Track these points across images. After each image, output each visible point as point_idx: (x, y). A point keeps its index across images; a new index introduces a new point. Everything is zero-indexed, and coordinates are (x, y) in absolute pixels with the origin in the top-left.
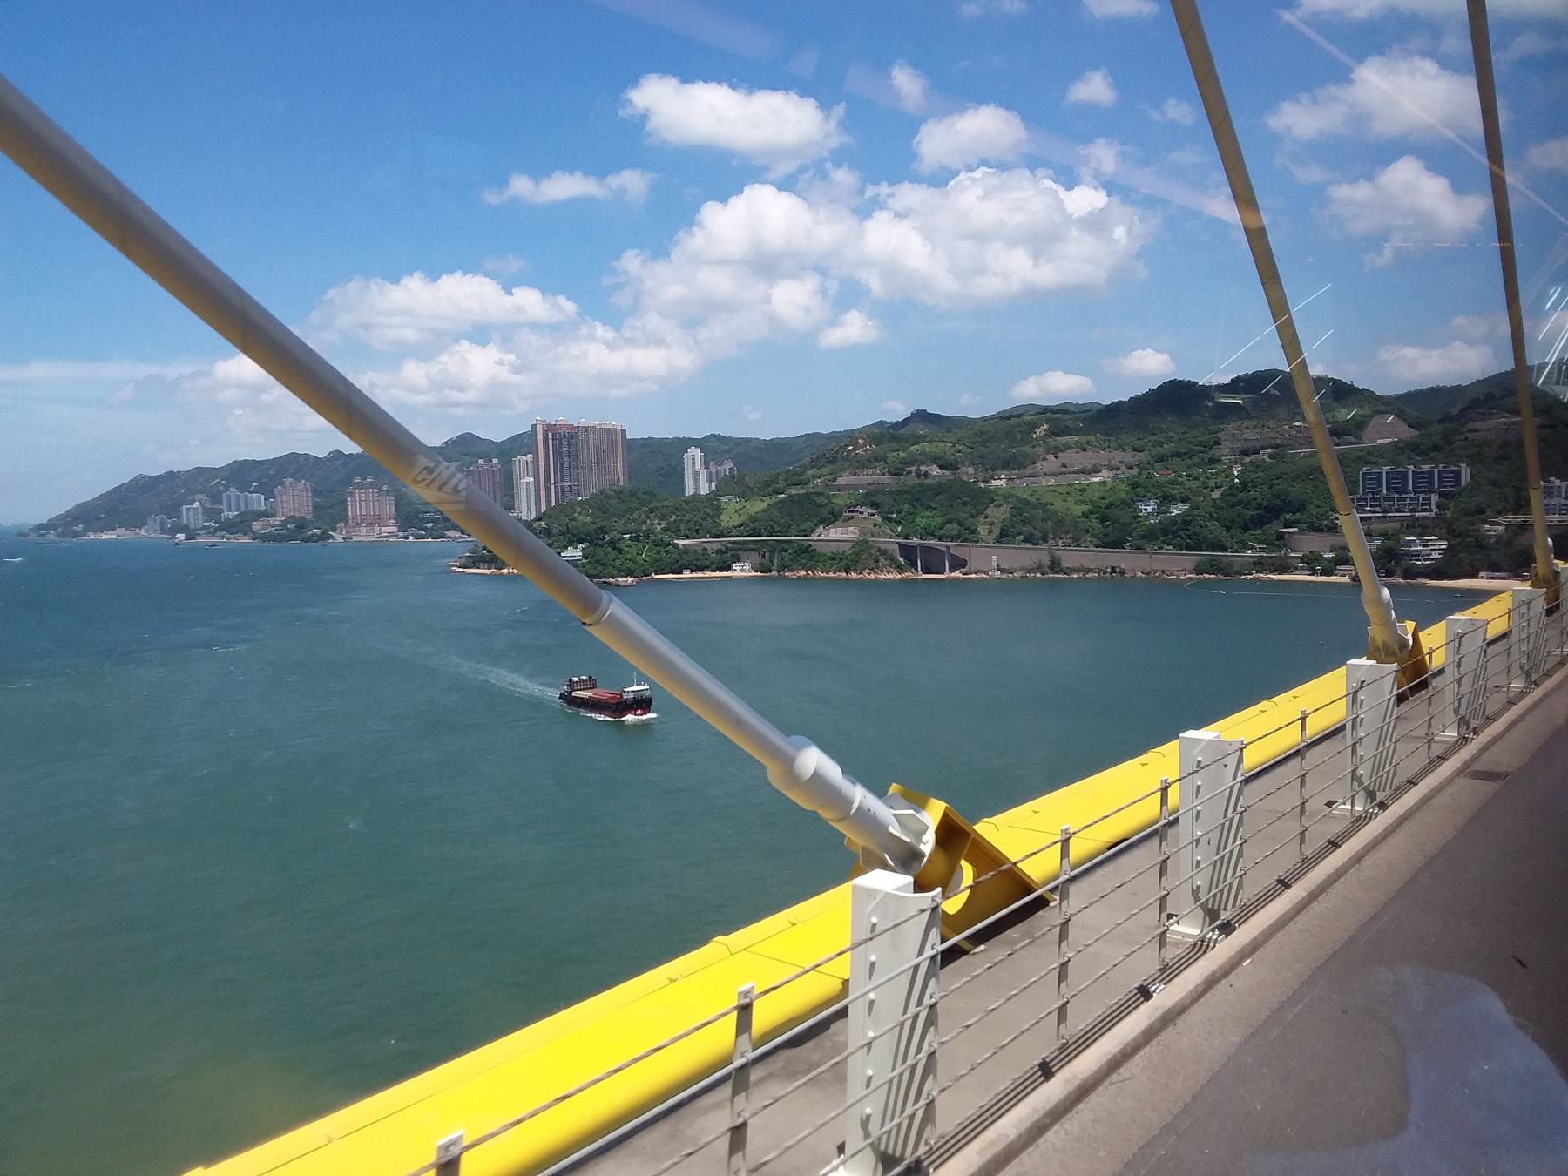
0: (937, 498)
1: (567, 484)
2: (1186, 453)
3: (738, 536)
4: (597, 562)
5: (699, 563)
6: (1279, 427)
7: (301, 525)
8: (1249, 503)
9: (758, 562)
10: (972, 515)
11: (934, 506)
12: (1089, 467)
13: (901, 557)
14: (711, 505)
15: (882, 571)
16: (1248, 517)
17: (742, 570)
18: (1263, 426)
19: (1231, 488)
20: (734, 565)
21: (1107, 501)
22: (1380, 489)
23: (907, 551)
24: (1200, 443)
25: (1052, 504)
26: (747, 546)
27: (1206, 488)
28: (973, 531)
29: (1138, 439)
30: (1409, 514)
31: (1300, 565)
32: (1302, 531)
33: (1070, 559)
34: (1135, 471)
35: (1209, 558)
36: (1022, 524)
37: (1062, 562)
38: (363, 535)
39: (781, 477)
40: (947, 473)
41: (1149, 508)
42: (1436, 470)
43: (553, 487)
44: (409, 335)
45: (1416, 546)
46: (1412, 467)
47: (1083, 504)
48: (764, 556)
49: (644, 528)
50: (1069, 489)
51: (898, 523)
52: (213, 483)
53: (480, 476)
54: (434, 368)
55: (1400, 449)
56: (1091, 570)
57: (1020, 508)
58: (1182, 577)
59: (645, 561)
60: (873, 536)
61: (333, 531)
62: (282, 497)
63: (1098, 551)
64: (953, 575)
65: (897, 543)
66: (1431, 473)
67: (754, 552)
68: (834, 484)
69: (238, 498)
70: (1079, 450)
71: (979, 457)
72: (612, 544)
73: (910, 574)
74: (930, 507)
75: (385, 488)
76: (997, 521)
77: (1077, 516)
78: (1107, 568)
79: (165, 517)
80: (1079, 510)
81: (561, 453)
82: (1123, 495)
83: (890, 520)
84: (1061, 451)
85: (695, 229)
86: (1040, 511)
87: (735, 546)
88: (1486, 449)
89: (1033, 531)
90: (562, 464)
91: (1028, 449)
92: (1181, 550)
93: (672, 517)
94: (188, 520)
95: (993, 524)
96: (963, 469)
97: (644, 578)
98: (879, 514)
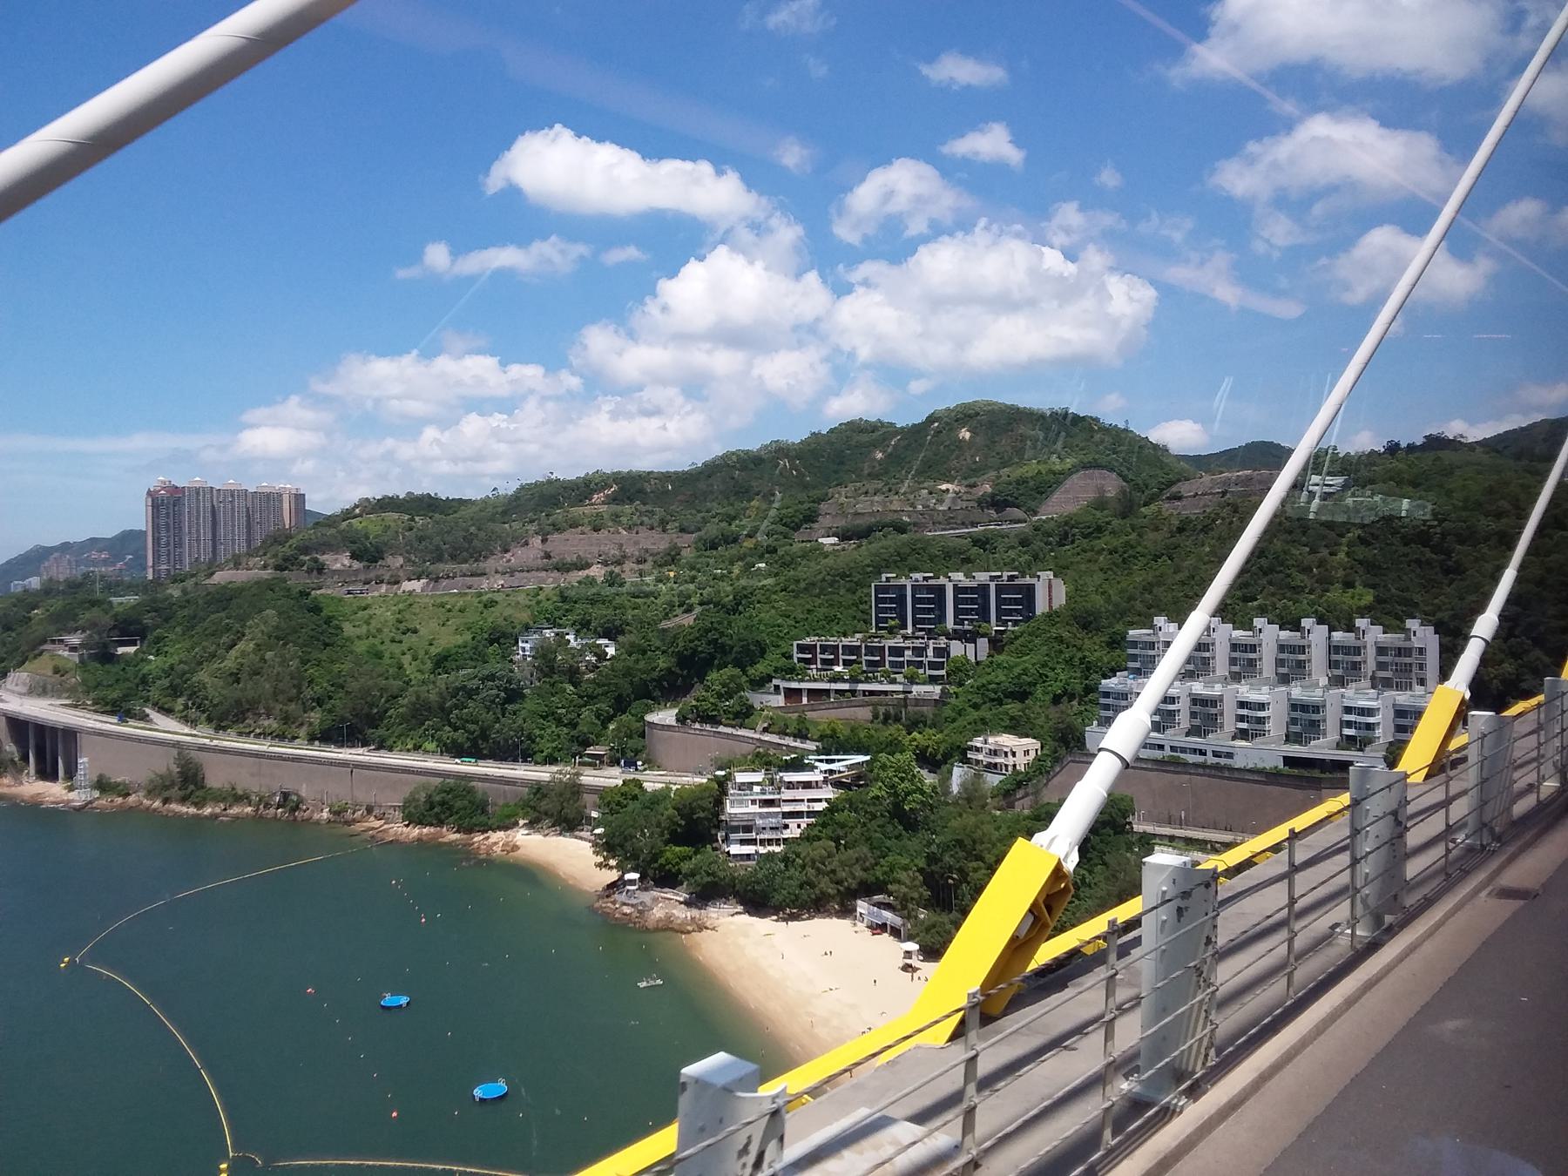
18: (890, 490)
25: (415, 631)
30: (899, 688)
41: (527, 646)
42: (993, 585)
44: (416, 407)
46: (958, 576)
66: (983, 589)
68: (207, 582)
78: (275, 794)
83: (106, 657)
88: (1151, 535)
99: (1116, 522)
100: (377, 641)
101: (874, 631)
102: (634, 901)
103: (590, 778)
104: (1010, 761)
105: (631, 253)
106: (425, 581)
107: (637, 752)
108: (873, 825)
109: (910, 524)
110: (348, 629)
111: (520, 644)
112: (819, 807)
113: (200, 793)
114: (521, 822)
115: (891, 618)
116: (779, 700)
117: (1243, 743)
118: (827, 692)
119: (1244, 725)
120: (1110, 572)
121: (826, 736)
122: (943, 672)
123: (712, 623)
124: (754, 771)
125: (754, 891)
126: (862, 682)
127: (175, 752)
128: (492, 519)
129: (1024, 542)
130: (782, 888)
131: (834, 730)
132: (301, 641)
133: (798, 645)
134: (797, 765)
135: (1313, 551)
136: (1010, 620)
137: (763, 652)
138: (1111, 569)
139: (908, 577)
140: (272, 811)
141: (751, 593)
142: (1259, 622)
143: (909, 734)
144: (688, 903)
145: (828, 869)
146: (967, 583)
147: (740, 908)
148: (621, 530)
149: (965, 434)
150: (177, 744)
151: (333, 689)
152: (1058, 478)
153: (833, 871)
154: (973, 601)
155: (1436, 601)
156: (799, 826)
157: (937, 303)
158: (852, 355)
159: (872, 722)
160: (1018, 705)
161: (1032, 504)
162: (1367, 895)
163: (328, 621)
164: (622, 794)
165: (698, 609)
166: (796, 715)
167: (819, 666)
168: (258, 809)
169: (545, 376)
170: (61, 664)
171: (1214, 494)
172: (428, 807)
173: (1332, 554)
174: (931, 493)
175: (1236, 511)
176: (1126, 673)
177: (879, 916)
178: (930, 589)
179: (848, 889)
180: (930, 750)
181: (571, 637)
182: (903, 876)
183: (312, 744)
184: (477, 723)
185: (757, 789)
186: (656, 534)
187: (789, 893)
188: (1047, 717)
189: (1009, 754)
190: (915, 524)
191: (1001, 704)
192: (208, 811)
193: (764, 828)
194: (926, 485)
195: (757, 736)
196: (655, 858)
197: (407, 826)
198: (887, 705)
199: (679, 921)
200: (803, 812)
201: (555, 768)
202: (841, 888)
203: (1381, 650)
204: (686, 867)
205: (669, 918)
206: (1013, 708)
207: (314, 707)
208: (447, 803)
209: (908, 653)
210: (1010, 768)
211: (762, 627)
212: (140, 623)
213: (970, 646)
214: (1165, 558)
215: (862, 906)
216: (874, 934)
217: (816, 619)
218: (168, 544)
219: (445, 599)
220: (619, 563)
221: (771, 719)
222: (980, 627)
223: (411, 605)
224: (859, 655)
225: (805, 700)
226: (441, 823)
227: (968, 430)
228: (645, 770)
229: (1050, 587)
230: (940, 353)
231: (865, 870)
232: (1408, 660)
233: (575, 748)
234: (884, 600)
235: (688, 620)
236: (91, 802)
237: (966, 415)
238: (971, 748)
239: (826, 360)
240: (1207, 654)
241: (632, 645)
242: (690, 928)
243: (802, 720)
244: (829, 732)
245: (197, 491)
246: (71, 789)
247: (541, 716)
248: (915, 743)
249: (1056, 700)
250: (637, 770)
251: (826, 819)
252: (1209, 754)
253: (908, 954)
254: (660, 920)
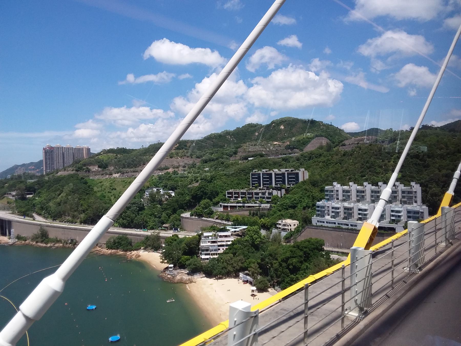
1: (48, 171)
6: (265, 145)
25: (115, 189)
30: (257, 205)
42: (286, 173)
44: (126, 122)
46: (276, 170)
66: (283, 174)
88: (335, 157)
99: (325, 153)
100: (104, 192)
101: (251, 187)
102: (172, 274)
103: (163, 234)
104: (289, 228)
105: (187, 76)
106: (120, 174)
107: (178, 226)
108: (245, 249)
109: (265, 154)
110: (95, 189)
111: (146, 193)
112: (229, 243)
113: (47, 240)
114: (142, 248)
115: (256, 183)
116: (221, 209)
117: (360, 222)
118: (236, 206)
119: (360, 216)
120: (322, 168)
121: (235, 220)
122: (270, 200)
123: (202, 186)
124: (210, 232)
125: (208, 270)
126: (246, 203)
127: (40, 227)
128: (140, 155)
129: (298, 159)
130: (216, 269)
131: (237, 219)
132: (79, 193)
133: (227, 192)
134: (224, 230)
135: (383, 161)
136: (291, 184)
137: (218, 195)
138: (323, 167)
139: (261, 171)
140: (68, 245)
141: (216, 176)
142: (365, 184)
143: (260, 219)
144: (188, 274)
145: (231, 263)
146: (279, 172)
147: (204, 275)
148: (178, 157)
149: (282, 127)
150: (40, 225)
151: (88, 207)
152: (309, 140)
153: (232, 264)
154: (280, 178)
155: (421, 176)
156: (223, 249)
157: (278, 89)
158: (253, 105)
159: (249, 216)
160: (293, 210)
161: (302, 148)
162: (357, 300)
163: (89, 187)
164: (172, 239)
165: (200, 181)
166: (226, 214)
167: (234, 199)
168: (64, 245)
169: (163, 112)
170: (9, 200)
171: (355, 144)
172: (114, 243)
173: (389, 162)
174: (271, 145)
175: (360, 149)
176: (325, 200)
177: (246, 278)
178: (268, 174)
179: (237, 269)
180: (266, 224)
181: (161, 190)
182: (252, 265)
183: (81, 224)
184: (129, 217)
185: (210, 238)
186: (189, 159)
187: (218, 271)
188: (301, 214)
189: (289, 226)
190: (266, 154)
191: (287, 210)
192: (49, 245)
193: (212, 250)
194: (270, 143)
195: (214, 220)
196: (178, 260)
197: (107, 249)
198: (253, 210)
199: (185, 280)
200: (224, 245)
201: (153, 231)
202: (235, 269)
203: (403, 192)
204: (187, 263)
205: (182, 279)
206: (291, 211)
207: (82, 213)
208: (120, 242)
209: (260, 194)
210: (289, 230)
211: (218, 187)
212: (34, 188)
213: (279, 192)
214: (338, 164)
215: (241, 275)
216: (244, 284)
217: (234, 184)
218: (49, 164)
219: (125, 179)
220: (178, 168)
221: (219, 215)
222: (282, 186)
223: (114, 181)
224: (246, 195)
225: (229, 209)
226: (118, 249)
228: (180, 231)
229: (303, 173)
230: (279, 104)
231: (242, 263)
232: (411, 195)
233: (160, 225)
234: (254, 178)
235: (196, 185)
236: (15, 243)
237: (282, 121)
238: (278, 224)
239: (246, 106)
240: (349, 194)
241: (179, 193)
242: (188, 282)
243: (227, 215)
244: (236, 219)
245: (58, 148)
246: (10, 239)
247: (150, 215)
248: (262, 222)
249: (304, 208)
250: (178, 231)
251: (231, 247)
252: (350, 225)
253: (253, 291)
254: (179, 279)
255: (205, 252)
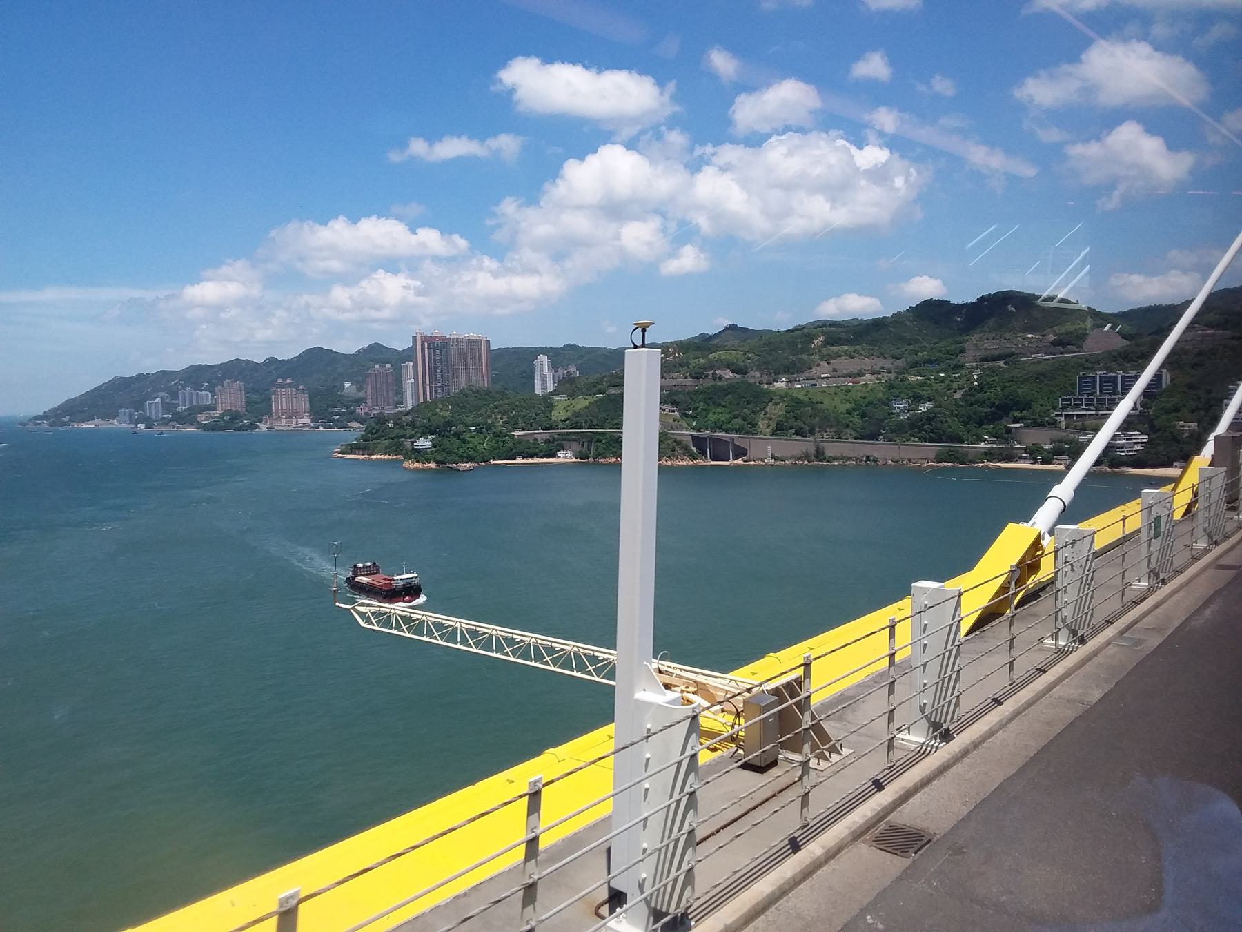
0: (727, 397)
2: (937, 360)
3: (564, 429)
4: (444, 450)
5: (529, 451)
7: (235, 416)
8: (984, 401)
9: (578, 450)
10: (753, 412)
11: (723, 404)
12: (856, 372)
13: (694, 446)
14: (547, 403)
15: (677, 459)
16: (984, 414)
17: (565, 457)
19: (970, 389)
20: (558, 453)
21: (867, 400)
22: (1095, 391)
23: (698, 441)
24: (948, 352)
25: (822, 403)
26: (570, 437)
27: (950, 389)
28: (754, 425)
29: (898, 349)
31: (1024, 455)
32: (1026, 426)
33: (831, 449)
34: (893, 376)
35: (948, 448)
36: (793, 420)
37: (826, 452)
38: (283, 425)
39: (605, 379)
40: (738, 376)
43: (428, 387)
44: (335, 265)
45: (1120, 440)
47: (848, 403)
48: (583, 445)
49: (489, 421)
50: (837, 390)
51: (694, 418)
52: (173, 383)
53: (376, 379)
54: (355, 292)
55: (1114, 357)
56: (849, 459)
57: (793, 406)
58: (926, 465)
59: (485, 449)
60: (672, 429)
61: (260, 422)
62: (221, 395)
63: (856, 443)
64: (736, 462)
65: (691, 435)
67: (575, 443)
69: (191, 395)
70: (847, 358)
71: (764, 363)
72: (457, 435)
73: (700, 461)
74: (720, 405)
75: (301, 388)
76: (774, 417)
77: (842, 413)
78: (863, 457)
79: (133, 410)
80: (844, 407)
81: (435, 360)
82: (880, 395)
83: (686, 415)
84: (832, 358)
85: (558, 181)
86: (810, 408)
87: (560, 437)
89: (803, 426)
90: (435, 368)
91: (805, 357)
92: (925, 442)
93: (512, 412)
94: (150, 413)
95: (770, 419)
96: (752, 373)
97: (483, 464)
98: (679, 410)
118: (1085, 415)
174: (1024, 339)
218: (442, 371)
224: (1094, 401)
225: (1075, 418)
227: (1012, 307)
249: (1193, 411)
255: (1121, 450)
